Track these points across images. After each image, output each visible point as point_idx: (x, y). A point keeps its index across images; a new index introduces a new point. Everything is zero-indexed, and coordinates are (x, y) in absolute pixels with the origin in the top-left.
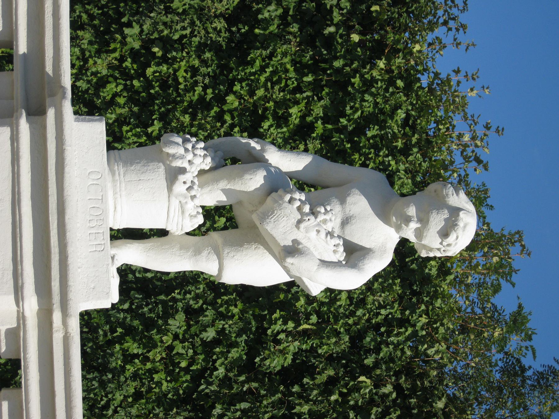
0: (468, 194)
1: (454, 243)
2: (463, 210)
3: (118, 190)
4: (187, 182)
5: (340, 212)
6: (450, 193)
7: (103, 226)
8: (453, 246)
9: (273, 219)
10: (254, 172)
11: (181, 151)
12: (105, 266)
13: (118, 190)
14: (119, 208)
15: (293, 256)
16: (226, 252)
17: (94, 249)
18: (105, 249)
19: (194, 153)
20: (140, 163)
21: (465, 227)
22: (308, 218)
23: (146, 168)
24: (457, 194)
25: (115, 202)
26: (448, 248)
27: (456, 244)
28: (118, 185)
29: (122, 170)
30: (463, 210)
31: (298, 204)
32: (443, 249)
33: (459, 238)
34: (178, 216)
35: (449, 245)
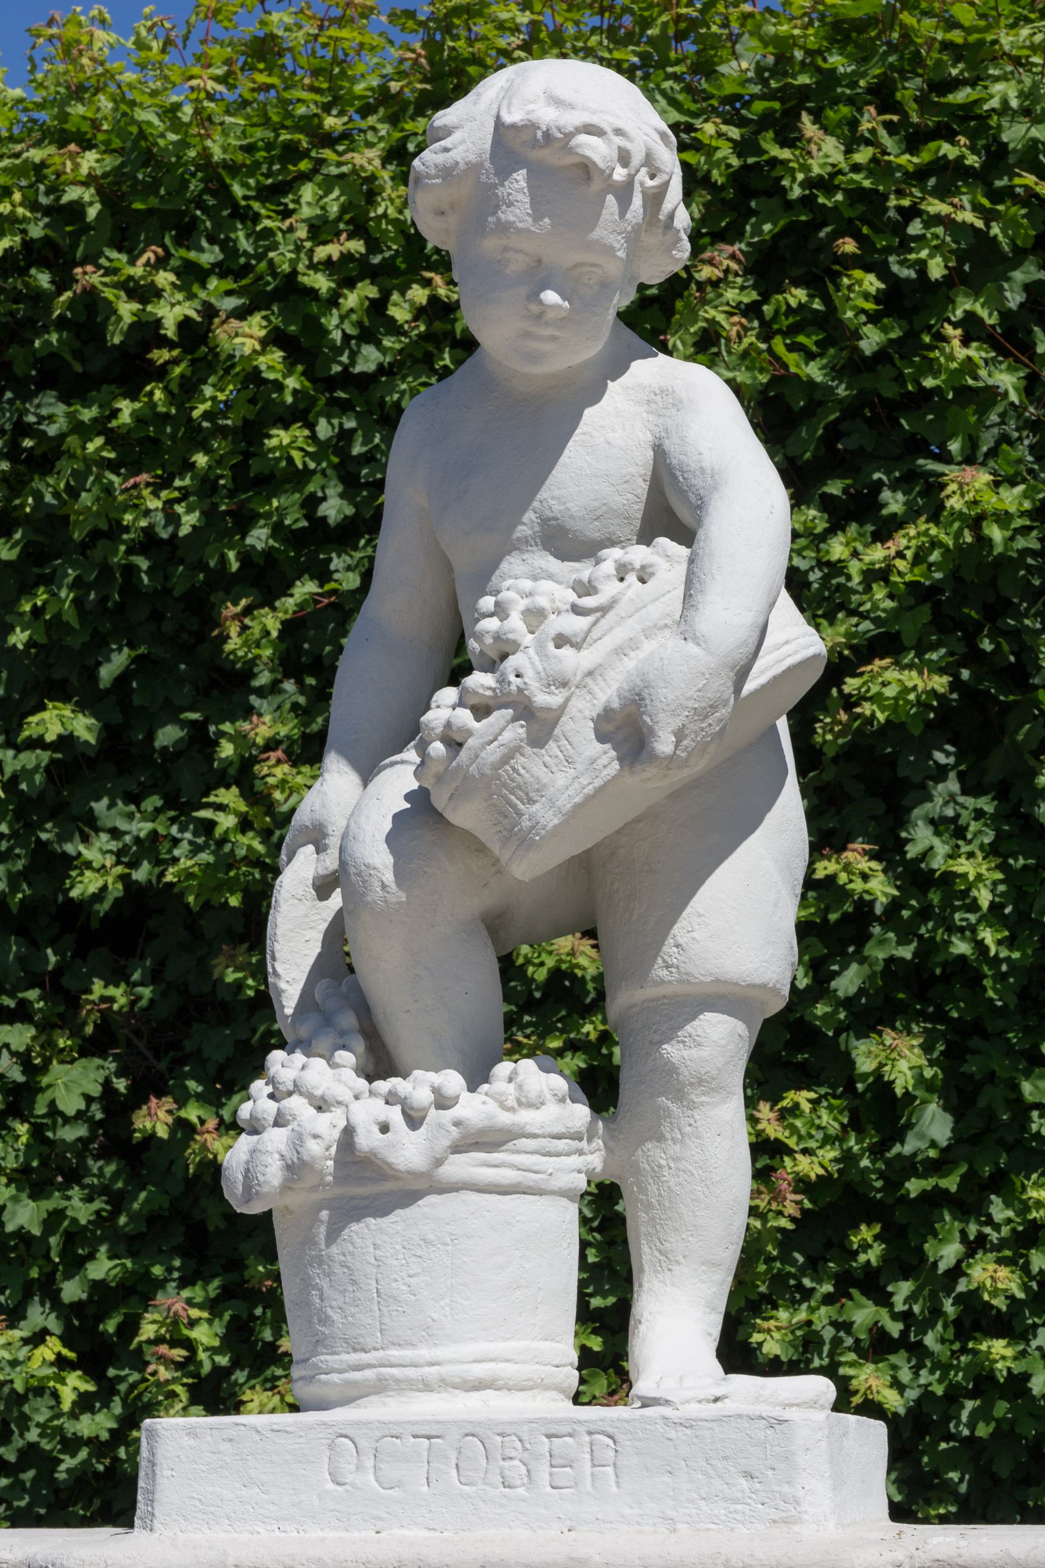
0: (443, 101)
1: (618, 141)
2: (498, 118)
3: (369, 1374)
4: (382, 1118)
5: (526, 556)
6: (441, 159)
7: (525, 1437)
8: (628, 145)
9: (521, 806)
10: (359, 874)
11: (276, 1139)
12: (673, 1434)
13: (411, 1372)
14: (480, 1371)
15: (652, 732)
16: (663, 973)
17: (610, 1470)
18: (610, 1430)
19: (290, 1094)
20: (321, 1290)
21: (557, 102)
22: (512, 678)
23: (338, 1270)
24: (447, 131)
25: (456, 1387)
26: (637, 158)
27: (619, 132)
28: (394, 1371)
29: (345, 1357)
30: (498, 118)
31: (465, 716)
32: (643, 175)
33: (594, 120)
34: (518, 1152)
35: (624, 158)
